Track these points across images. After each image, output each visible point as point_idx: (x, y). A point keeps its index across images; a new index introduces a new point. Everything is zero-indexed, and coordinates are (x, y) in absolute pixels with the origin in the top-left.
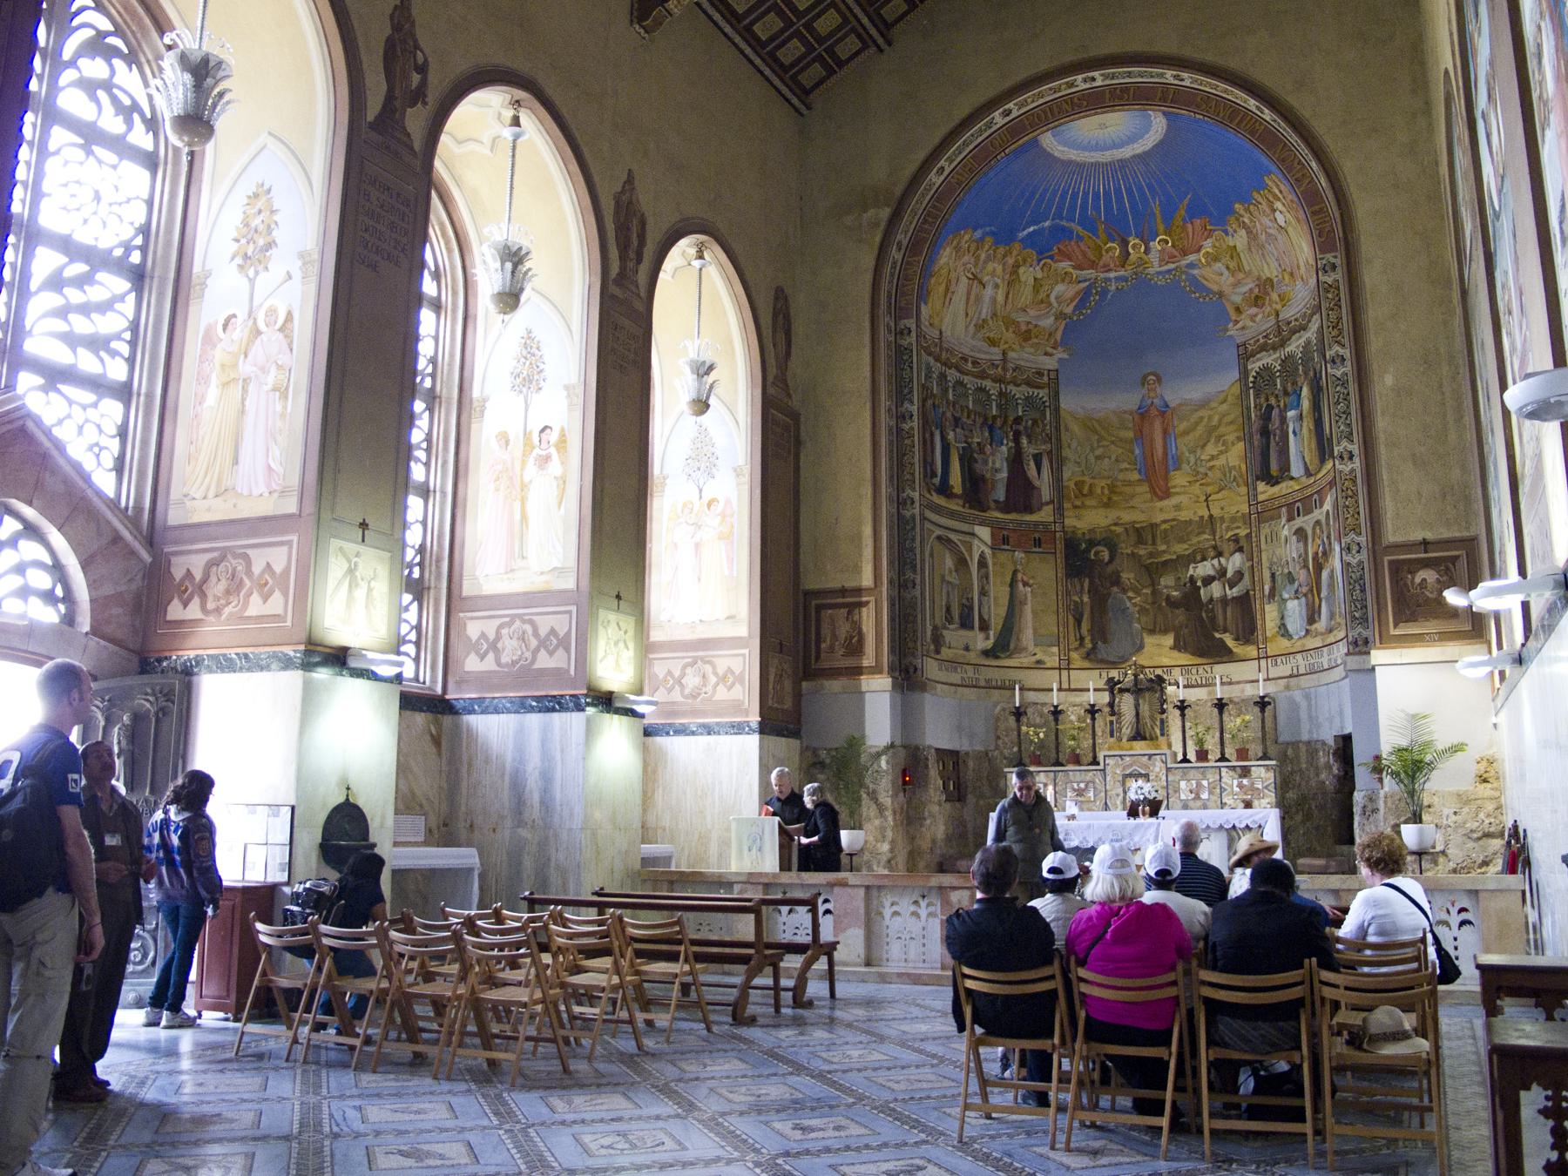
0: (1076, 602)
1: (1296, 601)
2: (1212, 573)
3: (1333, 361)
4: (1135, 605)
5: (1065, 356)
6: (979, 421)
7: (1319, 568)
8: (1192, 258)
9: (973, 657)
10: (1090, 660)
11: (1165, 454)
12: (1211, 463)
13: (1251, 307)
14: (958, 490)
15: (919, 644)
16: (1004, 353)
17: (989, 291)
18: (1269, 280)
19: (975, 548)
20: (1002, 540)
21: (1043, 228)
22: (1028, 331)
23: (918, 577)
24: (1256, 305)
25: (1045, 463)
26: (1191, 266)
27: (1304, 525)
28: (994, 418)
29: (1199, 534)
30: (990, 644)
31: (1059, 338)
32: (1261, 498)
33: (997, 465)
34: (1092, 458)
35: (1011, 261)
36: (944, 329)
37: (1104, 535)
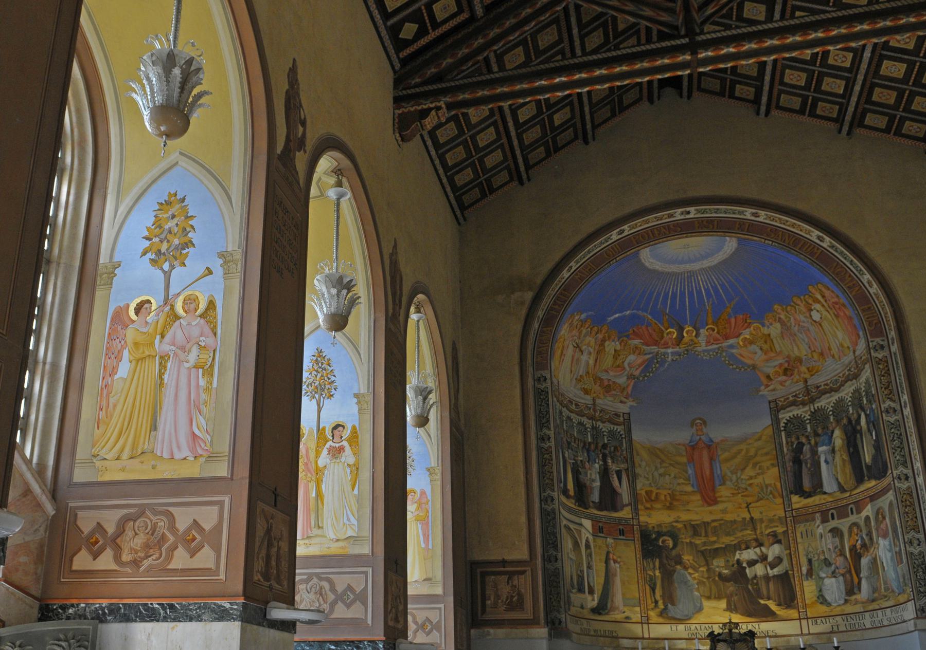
20: (599, 530)
37: (669, 529)
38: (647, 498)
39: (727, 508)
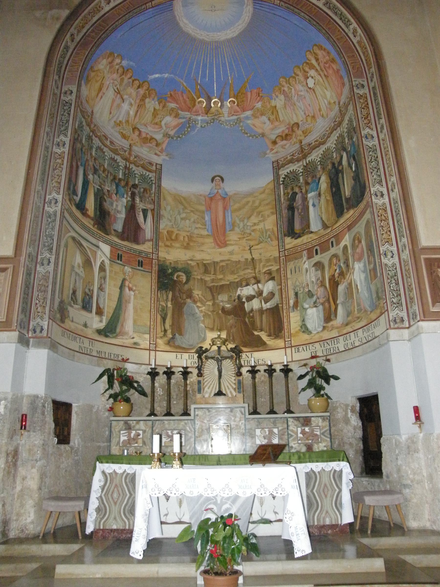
0: (163, 306)
1: (315, 309)
2: (253, 293)
3: (366, 137)
4: (201, 311)
6: (110, 178)
7: (335, 284)
9: (90, 332)
11: (224, 221)
13: (282, 140)
16: (130, 145)
17: (125, 106)
18: (297, 124)
19: (98, 256)
22: (146, 138)
23: (53, 257)
24: (286, 139)
26: (247, 118)
27: (323, 260)
28: (120, 180)
30: (102, 325)
32: (287, 247)
33: (119, 208)
34: (178, 217)
35: (142, 91)
36: (94, 111)
37: (183, 266)
38: (168, 238)
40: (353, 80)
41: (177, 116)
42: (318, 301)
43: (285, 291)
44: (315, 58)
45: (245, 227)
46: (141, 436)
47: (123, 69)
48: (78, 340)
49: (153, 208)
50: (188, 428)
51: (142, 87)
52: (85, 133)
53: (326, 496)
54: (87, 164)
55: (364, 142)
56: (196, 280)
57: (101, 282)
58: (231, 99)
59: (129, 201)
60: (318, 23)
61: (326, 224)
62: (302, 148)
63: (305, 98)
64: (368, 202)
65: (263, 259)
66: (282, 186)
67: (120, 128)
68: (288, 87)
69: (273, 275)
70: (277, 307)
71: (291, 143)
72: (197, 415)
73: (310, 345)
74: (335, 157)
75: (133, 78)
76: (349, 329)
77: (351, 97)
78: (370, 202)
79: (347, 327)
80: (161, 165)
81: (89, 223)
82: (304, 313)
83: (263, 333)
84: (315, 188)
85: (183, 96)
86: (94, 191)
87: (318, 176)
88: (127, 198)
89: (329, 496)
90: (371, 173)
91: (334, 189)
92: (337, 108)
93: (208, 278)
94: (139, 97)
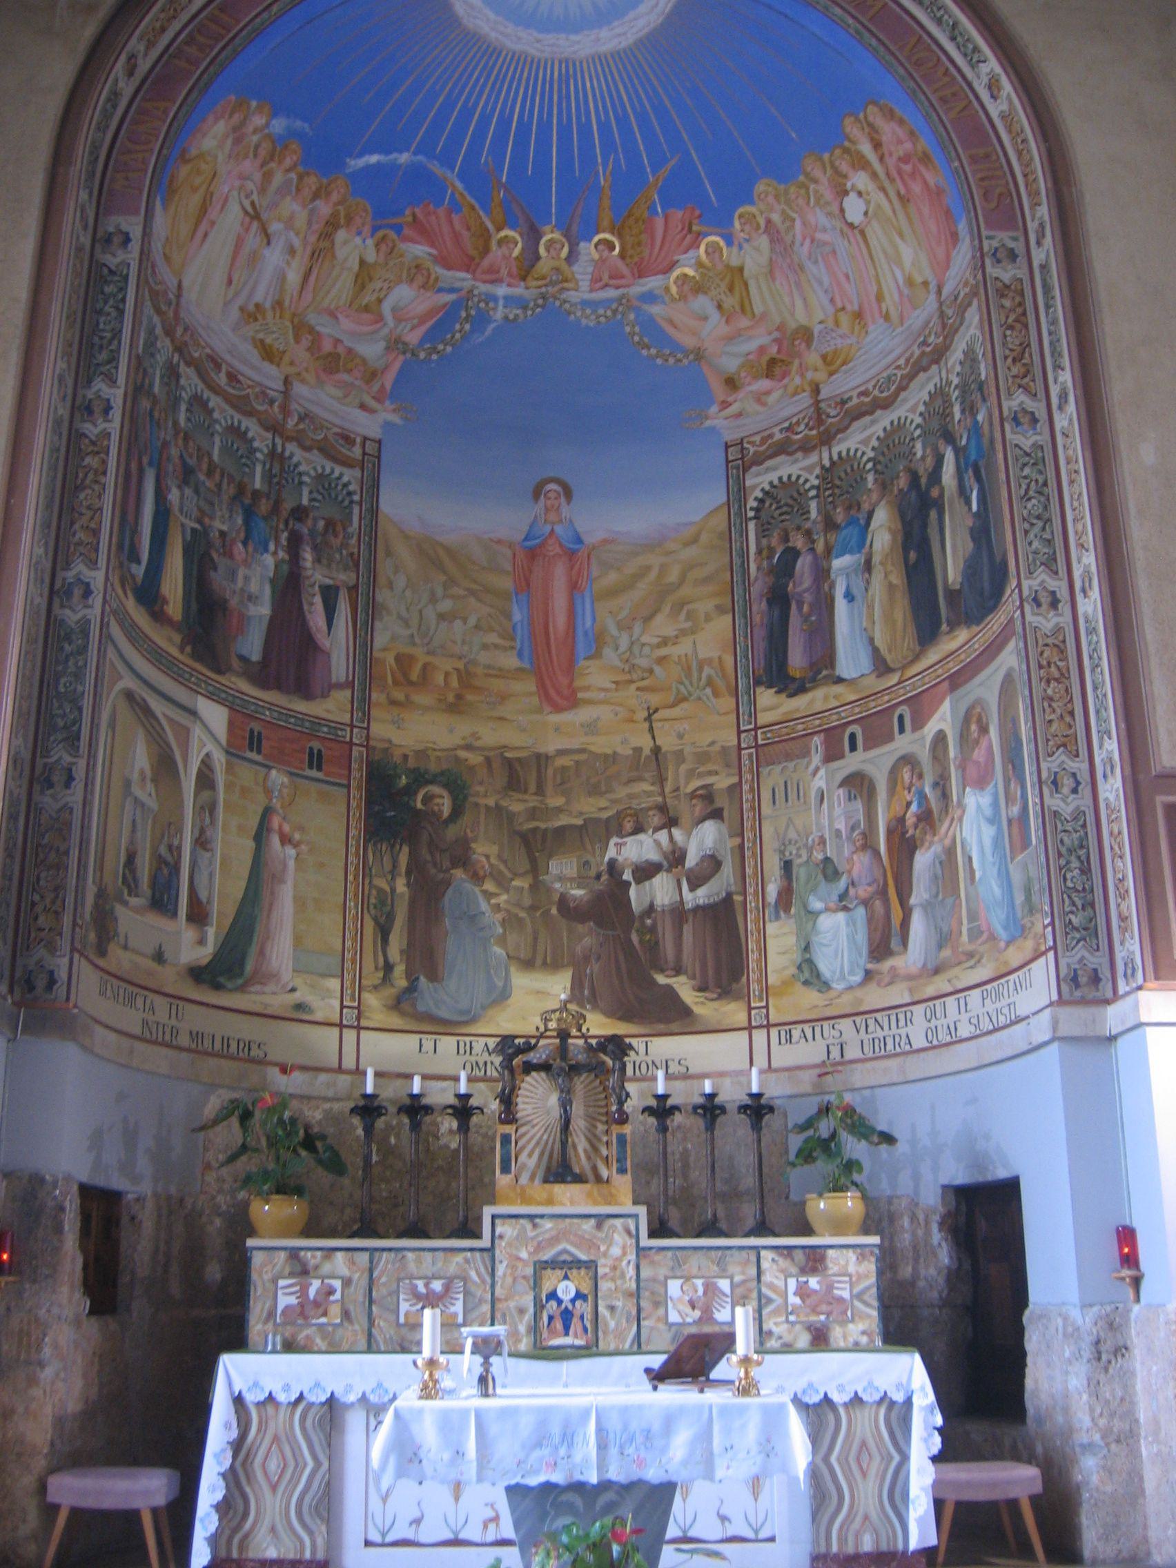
0: (380, 890)
1: (841, 916)
2: (654, 856)
3: (1016, 420)
4: (497, 908)
5: (395, 419)
6: (229, 490)
8: (653, 283)
9: (170, 978)
10: (403, 1014)
12: (663, 652)
14: (174, 609)
15: (67, 920)
16: (286, 381)
17: (273, 257)
18: (806, 335)
21: (394, 167)
22: (334, 357)
23: (82, 763)
24: (769, 374)
25: (343, 608)
26: (650, 297)
27: (870, 770)
28: (256, 494)
29: (631, 781)
30: (204, 954)
31: (388, 386)
32: (763, 718)
33: (254, 587)
34: (430, 614)
35: (324, 209)
36: (185, 284)
37: (445, 766)
39: (598, 718)
40: (984, 233)
41: (430, 284)
42: (852, 891)
43: (754, 854)
44: (872, 139)
45: (636, 649)
46: (338, 1296)
47: (273, 142)
48: (140, 1001)
49: (352, 583)
50: (473, 1274)
51: (328, 194)
52: (161, 359)
53: (864, 1474)
54: (164, 456)
55: (1009, 435)
56: (483, 810)
57: (203, 821)
58: (602, 236)
59: (283, 561)
60: (883, 44)
61: (884, 661)
62: (819, 411)
63: (834, 252)
64: (1011, 621)
65: (688, 750)
66: (752, 526)
67: (256, 326)
68: (783, 212)
69: (718, 804)
70: (726, 903)
71: (785, 387)
72: (501, 1237)
73: (826, 1024)
74: (919, 454)
75: (300, 169)
76: (940, 984)
77: (977, 286)
78: (1018, 623)
79: (937, 978)
80: (380, 442)
81: (167, 641)
82: (810, 925)
83: (682, 979)
84: (853, 542)
85: (450, 222)
86: (184, 540)
87: (866, 507)
88: (275, 553)
89: (873, 1472)
90: (1026, 532)
91: (913, 555)
92: (931, 303)
93: (516, 806)
94: (315, 227)
